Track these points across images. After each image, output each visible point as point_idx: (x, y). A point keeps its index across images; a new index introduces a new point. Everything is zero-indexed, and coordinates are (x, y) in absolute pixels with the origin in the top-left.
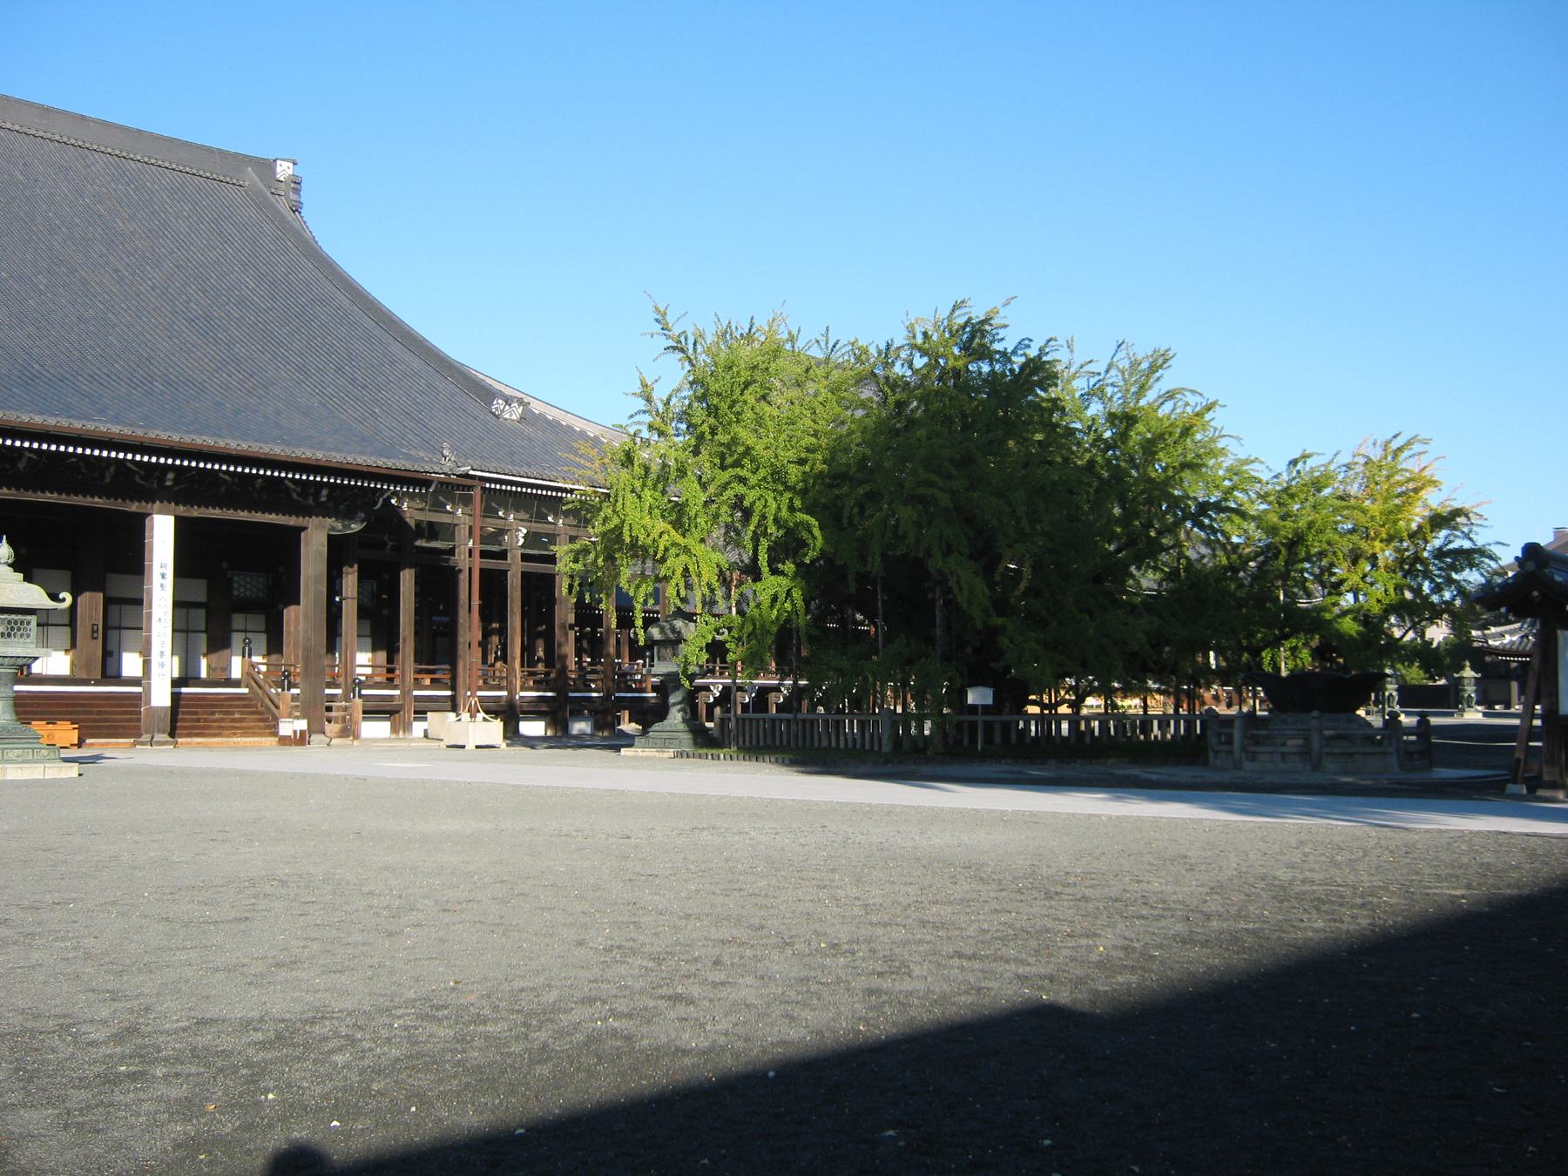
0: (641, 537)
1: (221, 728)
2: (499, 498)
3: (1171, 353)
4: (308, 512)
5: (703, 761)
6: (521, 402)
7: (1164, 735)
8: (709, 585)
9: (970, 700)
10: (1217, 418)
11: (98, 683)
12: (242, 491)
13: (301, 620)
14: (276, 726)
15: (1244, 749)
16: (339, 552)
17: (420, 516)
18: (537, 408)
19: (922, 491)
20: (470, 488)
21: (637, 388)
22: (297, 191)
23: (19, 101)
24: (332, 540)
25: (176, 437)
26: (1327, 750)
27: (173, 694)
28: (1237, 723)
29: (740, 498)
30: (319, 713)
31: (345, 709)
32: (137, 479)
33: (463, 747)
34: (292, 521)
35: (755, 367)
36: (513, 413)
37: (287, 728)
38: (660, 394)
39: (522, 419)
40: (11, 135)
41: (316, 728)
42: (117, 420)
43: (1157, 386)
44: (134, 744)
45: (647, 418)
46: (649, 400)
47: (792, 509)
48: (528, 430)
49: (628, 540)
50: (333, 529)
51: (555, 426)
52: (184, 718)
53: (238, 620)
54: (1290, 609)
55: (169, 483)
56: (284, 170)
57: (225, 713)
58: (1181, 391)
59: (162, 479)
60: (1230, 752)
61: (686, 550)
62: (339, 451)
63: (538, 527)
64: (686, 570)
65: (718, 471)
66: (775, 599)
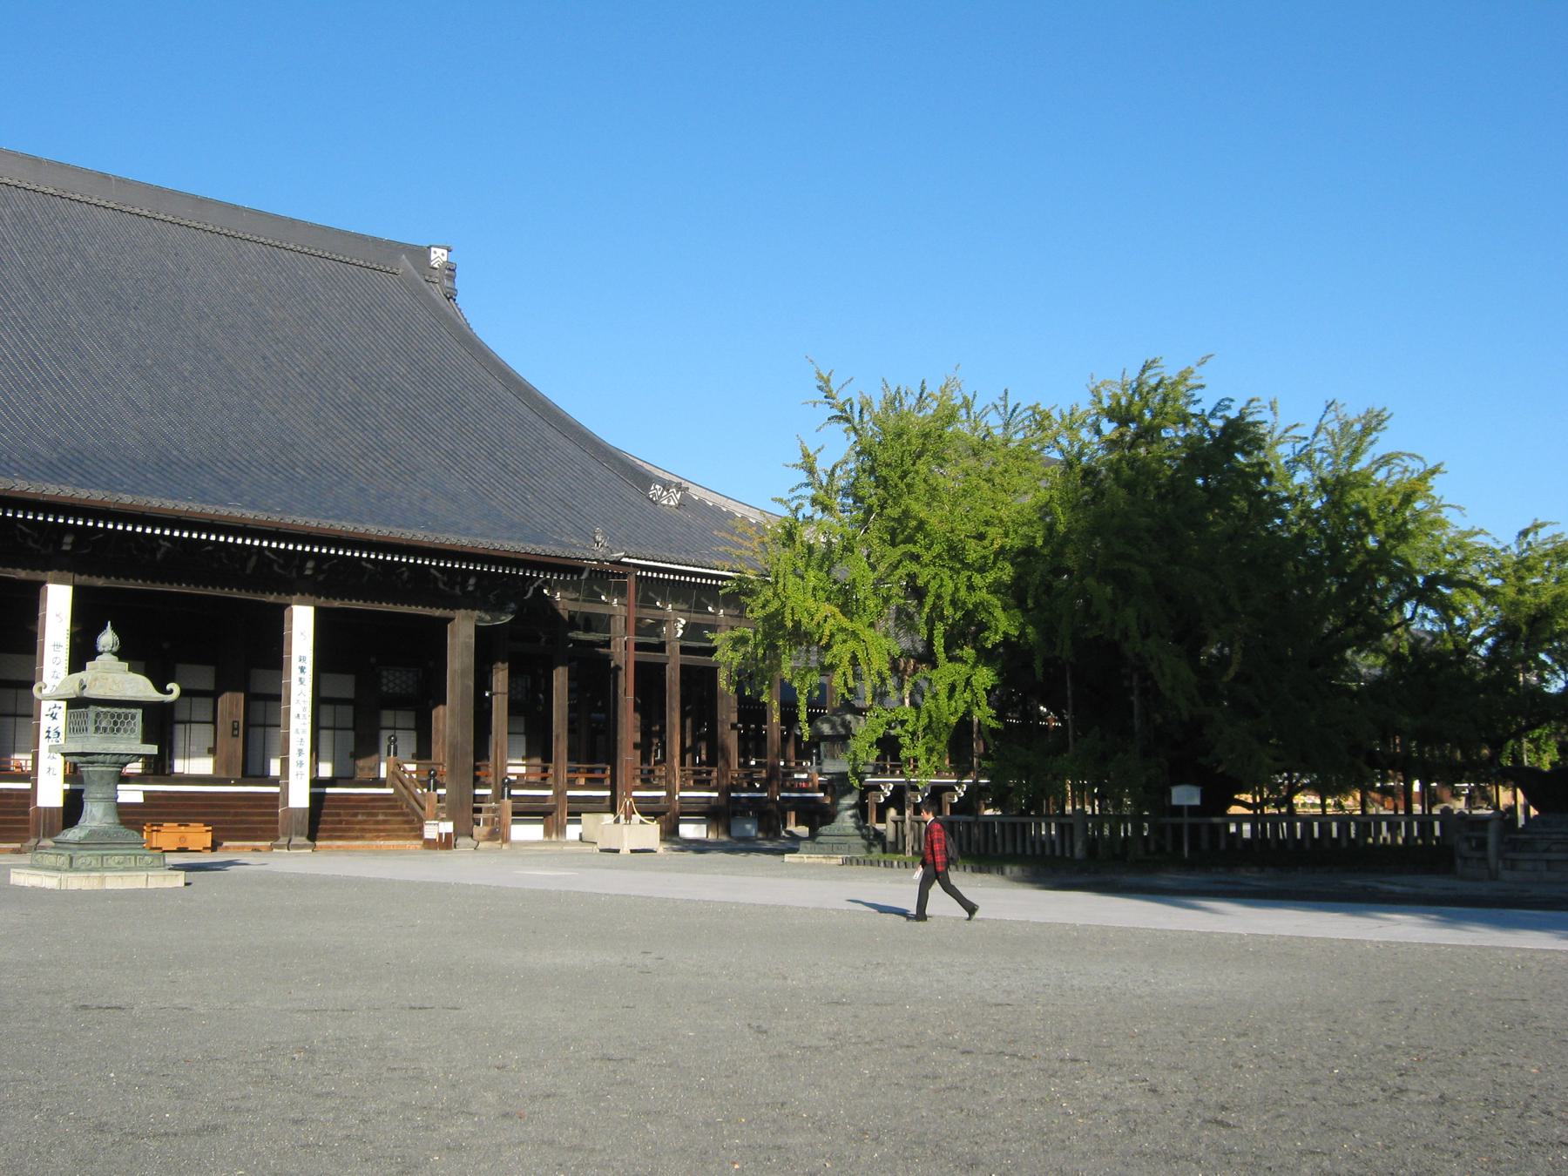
0: (805, 621)
1: (363, 830)
2: (654, 587)
3: (1386, 414)
4: (455, 605)
6: (679, 487)
7: (1394, 838)
8: (880, 674)
10: (1438, 486)
11: (238, 783)
12: (385, 580)
13: (450, 720)
14: (421, 829)
16: (487, 648)
17: (574, 607)
18: (696, 493)
20: (625, 576)
22: (452, 278)
23: (173, 192)
24: (480, 633)
25: (313, 523)
27: (312, 795)
28: (1492, 827)
30: (467, 814)
31: (495, 810)
32: (276, 568)
33: (617, 851)
34: (438, 613)
35: (926, 436)
37: (432, 830)
38: (823, 465)
39: (680, 505)
40: (165, 226)
41: (464, 830)
42: (252, 505)
43: (1372, 450)
44: (271, 848)
45: (810, 492)
46: (811, 471)
47: (971, 588)
49: (789, 624)
51: (715, 511)
52: (322, 820)
53: (387, 717)
54: (1536, 693)
55: (308, 572)
56: (438, 256)
57: (368, 814)
58: (1398, 455)
59: (302, 568)
60: (1484, 859)
63: (697, 618)
64: (854, 660)
66: (952, 689)
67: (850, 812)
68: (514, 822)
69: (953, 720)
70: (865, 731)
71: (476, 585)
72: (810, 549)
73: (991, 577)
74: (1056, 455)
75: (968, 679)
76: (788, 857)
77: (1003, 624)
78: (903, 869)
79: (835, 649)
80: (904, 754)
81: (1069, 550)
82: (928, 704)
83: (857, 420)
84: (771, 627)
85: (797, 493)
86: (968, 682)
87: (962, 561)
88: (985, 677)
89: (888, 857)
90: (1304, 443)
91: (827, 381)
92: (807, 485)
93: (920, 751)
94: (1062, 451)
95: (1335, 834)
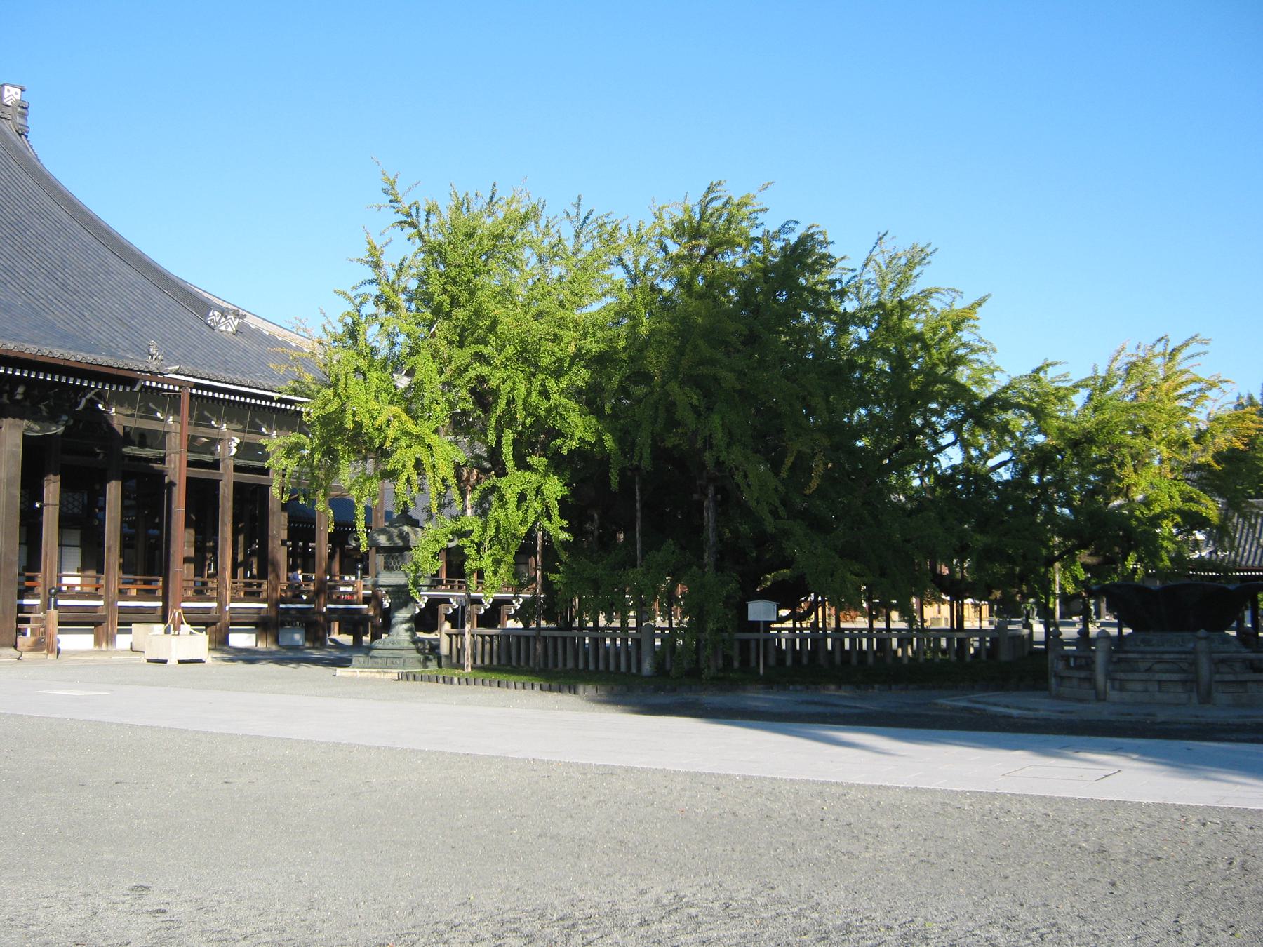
0: (367, 422)
2: (209, 405)
5: (433, 685)
6: (237, 315)
8: (444, 480)
9: (750, 618)
15: (1109, 676)
17: (130, 423)
18: (252, 322)
19: (703, 370)
21: (364, 254)
22: (24, 116)
24: (26, 438)
26: (1218, 677)
29: (481, 380)
31: (42, 620)
33: (165, 662)
35: (498, 237)
36: (229, 326)
38: (390, 260)
45: (374, 290)
46: (377, 265)
47: (545, 393)
48: (244, 342)
49: (350, 426)
50: (30, 429)
51: (271, 340)
60: (1090, 680)
61: (419, 438)
62: (32, 342)
63: (250, 437)
64: (418, 464)
65: (457, 350)
66: (522, 497)
67: (406, 626)
68: (60, 631)
69: (523, 531)
70: (427, 544)
71: (24, 394)
72: (374, 351)
73: (564, 382)
74: (619, 274)
75: (539, 487)
76: (340, 671)
77: (579, 428)
78: (464, 686)
79: (398, 455)
80: (469, 565)
81: (651, 354)
82: (496, 513)
83: (423, 224)
84: (328, 431)
85: (360, 291)
86: (538, 492)
87: (536, 365)
88: (555, 488)
89: (445, 671)
90: (851, 274)
91: (393, 184)
92: (372, 282)
93: (486, 563)
94: (626, 268)
95: (830, 647)
